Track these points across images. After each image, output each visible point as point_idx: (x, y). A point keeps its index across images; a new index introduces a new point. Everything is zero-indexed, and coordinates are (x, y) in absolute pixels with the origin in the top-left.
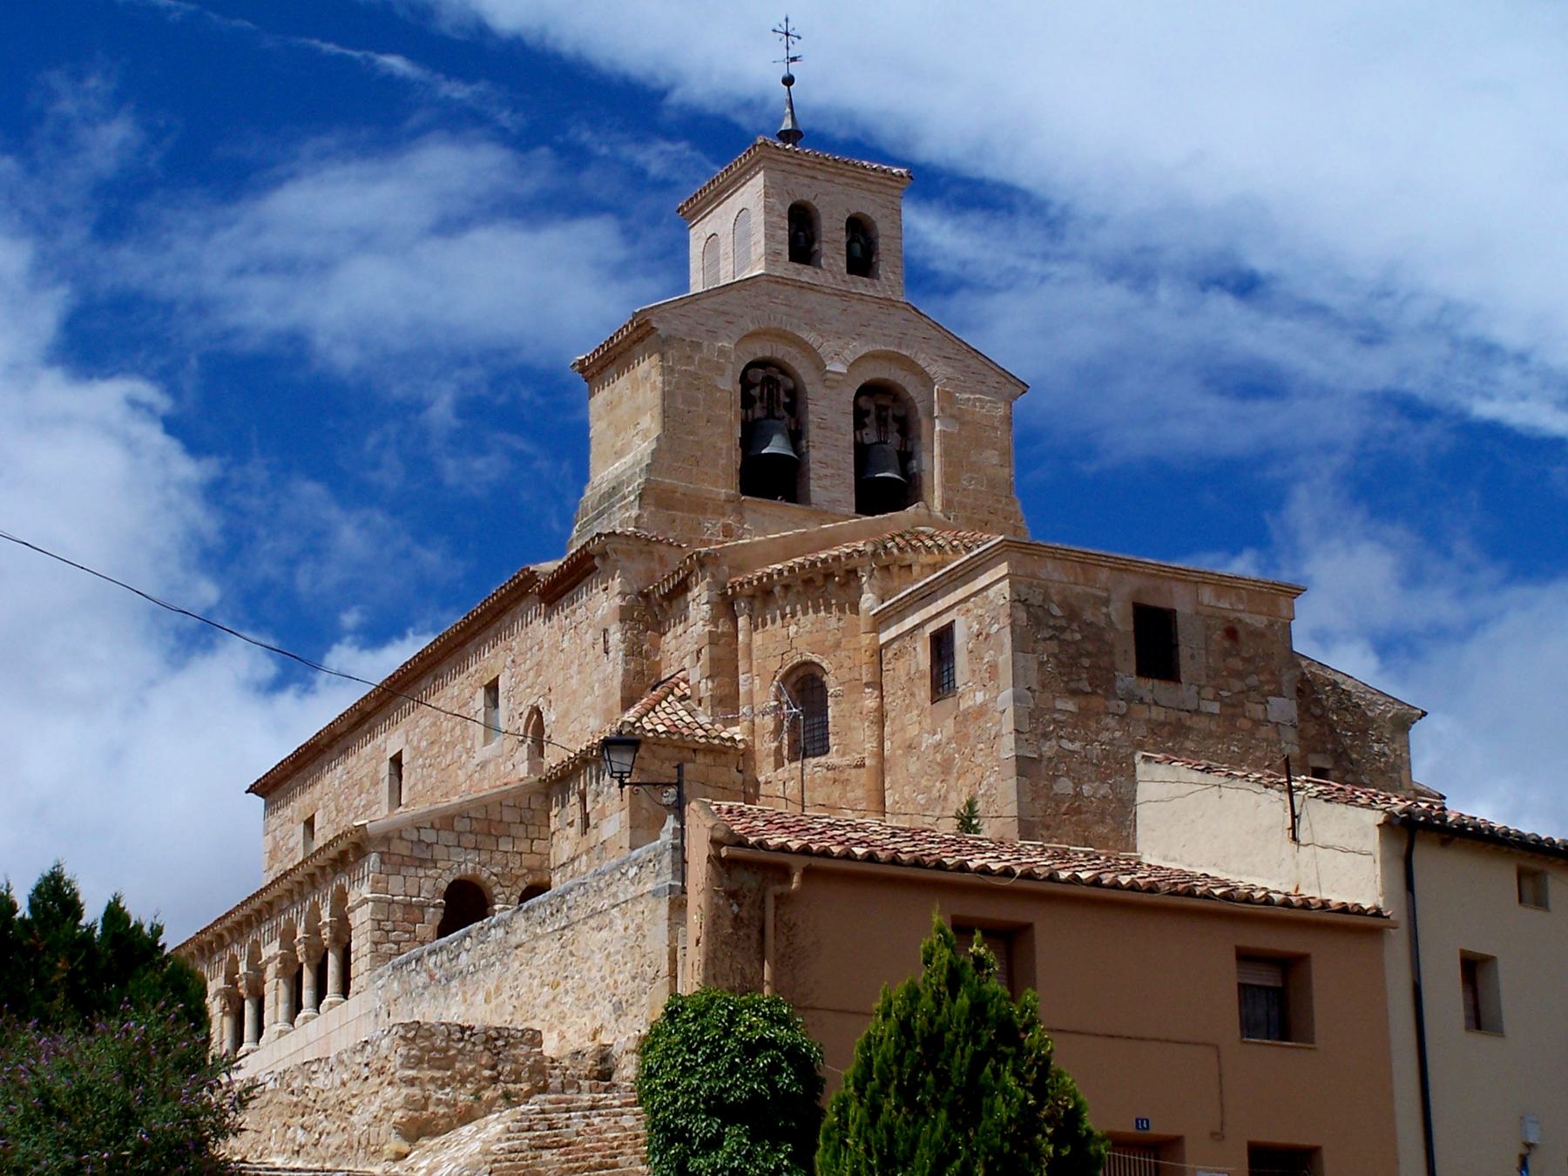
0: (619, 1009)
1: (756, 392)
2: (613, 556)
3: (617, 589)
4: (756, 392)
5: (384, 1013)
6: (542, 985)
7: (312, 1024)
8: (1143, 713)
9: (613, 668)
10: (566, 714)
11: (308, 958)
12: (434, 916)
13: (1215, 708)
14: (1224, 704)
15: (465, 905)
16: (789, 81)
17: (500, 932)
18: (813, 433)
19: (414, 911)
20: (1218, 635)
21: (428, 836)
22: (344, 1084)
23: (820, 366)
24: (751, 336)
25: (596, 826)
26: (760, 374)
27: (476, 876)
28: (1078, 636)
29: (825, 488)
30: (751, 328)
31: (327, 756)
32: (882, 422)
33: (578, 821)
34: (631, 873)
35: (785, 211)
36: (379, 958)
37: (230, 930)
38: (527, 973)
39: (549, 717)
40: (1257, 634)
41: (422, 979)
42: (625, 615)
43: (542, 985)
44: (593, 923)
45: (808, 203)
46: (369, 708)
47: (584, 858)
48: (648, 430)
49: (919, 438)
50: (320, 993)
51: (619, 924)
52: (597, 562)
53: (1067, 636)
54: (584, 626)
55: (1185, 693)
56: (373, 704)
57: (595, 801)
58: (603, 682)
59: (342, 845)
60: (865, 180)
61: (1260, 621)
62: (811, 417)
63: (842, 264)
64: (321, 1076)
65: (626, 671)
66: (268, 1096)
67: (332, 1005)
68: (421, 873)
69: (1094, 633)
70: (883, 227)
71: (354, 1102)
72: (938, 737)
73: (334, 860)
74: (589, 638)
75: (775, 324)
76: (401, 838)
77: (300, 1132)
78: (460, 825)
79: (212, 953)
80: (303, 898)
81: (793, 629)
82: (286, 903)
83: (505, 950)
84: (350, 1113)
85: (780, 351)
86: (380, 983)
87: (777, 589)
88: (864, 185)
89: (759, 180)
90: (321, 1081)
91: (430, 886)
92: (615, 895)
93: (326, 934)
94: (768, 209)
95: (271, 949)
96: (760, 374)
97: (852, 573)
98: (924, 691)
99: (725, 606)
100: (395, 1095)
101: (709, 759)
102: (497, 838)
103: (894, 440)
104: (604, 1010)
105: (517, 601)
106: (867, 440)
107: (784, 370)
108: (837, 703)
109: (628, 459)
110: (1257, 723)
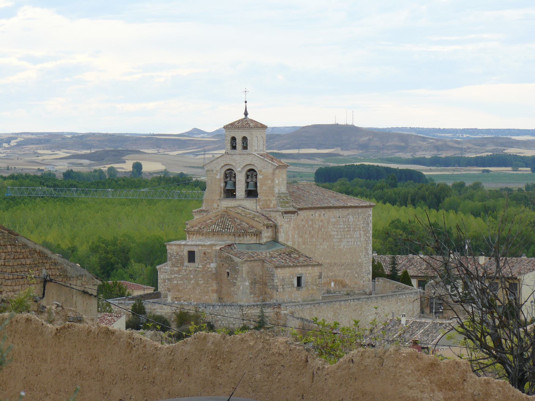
1: (228, 175)
4: (228, 175)
13: (201, 266)
14: (203, 265)
16: (246, 102)
32: (252, 177)
40: (209, 253)
55: (196, 265)
61: (210, 251)
69: (181, 257)
110: (208, 268)
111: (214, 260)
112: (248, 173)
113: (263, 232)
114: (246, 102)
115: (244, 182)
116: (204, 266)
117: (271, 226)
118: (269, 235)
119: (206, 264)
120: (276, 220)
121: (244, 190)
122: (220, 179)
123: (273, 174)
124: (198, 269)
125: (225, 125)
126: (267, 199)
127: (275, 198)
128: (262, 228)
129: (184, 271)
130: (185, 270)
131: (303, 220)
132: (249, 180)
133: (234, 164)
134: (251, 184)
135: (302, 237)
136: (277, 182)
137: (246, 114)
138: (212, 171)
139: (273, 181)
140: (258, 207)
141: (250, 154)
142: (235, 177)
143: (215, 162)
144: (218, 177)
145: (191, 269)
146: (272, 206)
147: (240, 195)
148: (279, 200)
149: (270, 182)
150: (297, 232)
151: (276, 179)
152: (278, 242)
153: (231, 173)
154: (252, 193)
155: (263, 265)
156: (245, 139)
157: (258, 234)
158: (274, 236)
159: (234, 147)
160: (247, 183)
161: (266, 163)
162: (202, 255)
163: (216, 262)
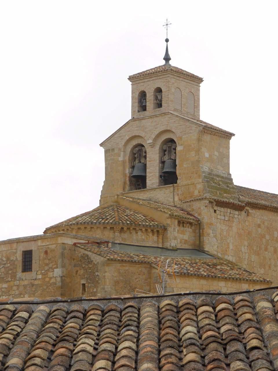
4: (136, 156)
8: (23, 283)
13: (40, 277)
14: (42, 274)
16: (167, 40)
28: (9, 265)
29: (150, 180)
53: (6, 266)
60: (158, 76)
61: (53, 247)
88: (158, 77)
110: (51, 278)
111: (60, 261)
113: (170, 229)
114: (167, 40)
115: (158, 161)
116: (45, 275)
117: (191, 224)
118: (186, 237)
119: (48, 270)
120: (200, 214)
122: (124, 162)
123: (199, 140)
124: (36, 282)
125: (132, 74)
126: (189, 182)
127: (200, 180)
128: (169, 221)
130: (18, 286)
131: (259, 226)
132: (166, 158)
133: (142, 134)
134: (168, 162)
135: (258, 254)
136: (207, 155)
137: (167, 58)
139: (198, 151)
140: (176, 199)
141: (165, 114)
142: (145, 157)
144: (121, 159)
145: (26, 283)
146: (196, 193)
147: (153, 184)
148: (207, 182)
149: (193, 154)
150: (246, 243)
151: (203, 149)
152: (204, 252)
153: (140, 150)
154: (169, 178)
155: (150, 273)
157: (160, 231)
158: (198, 242)
160: (163, 162)
161: (188, 124)
162: (42, 255)
163: (63, 266)
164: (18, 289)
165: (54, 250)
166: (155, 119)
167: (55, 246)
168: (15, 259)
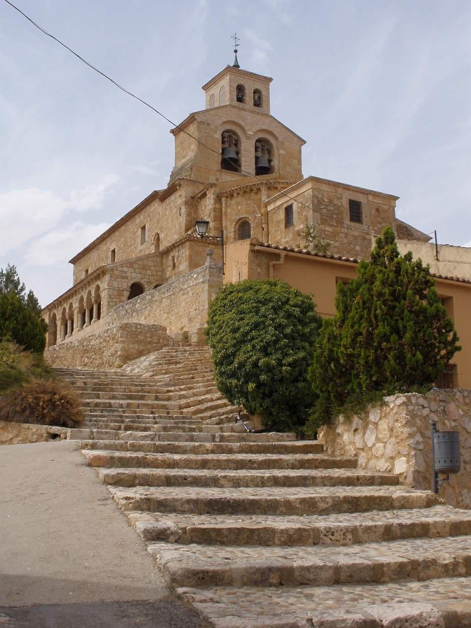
0: (190, 320)
1: (226, 139)
2: (183, 185)
3: (184, 196)
4: (226, 139)
5: (111, 324)
6: (164, 313)
7: (89, 327)
8: (351, 233)
9: (183, 220)
10: (167, 235)
11: (87, 308)
12: (126, 294)
15: (136, 290)
16: (236, 51)
17: (150, 297)
18: (243, 152)
19: (120, 292)
20: (373, 211)
21: (125, 269)
22: (101, 343)
23: (244, 131)
24: (224, 123)
25: (178, 267)
26: (227, 134)
27: (140, 282)
28: (332, 208)
30: (225, 120)
31: (93, 251)
32: (263, 150)
33: (172, 266)
34: (195, 276)
35: (236, 87)
36: (110, 306)
37: (64, 300)
38: (159, 309)
39: (162, 236)
40: (384, 211)
41: (124, 312)
42: (186, 203)
43: (164, 313)
44: (181, 293)
45: (242, 85)
46: (105, 236)
47: (174, 277)
48: (194, 149)
49: (274, 155)
50: (91, 318)
51: (191, 294)
52: (178, 188)
54: (173, 207)
56: (107, 235)
57: (178, 259)
58: (179, 224)
59: (98, 272)
61: (386, 207)
62: (242, 148)
63: (252, 103)
64: (93, 341)
65: (186, 220)
66: (76, 348)
67: (95, 321)
68: (123, 280)
69: (338, 207)
70: (264, 93)
71: (105, 349)
72: (287, 239)
73: (96, 277)
74: (174, 211)
75: (232, 119)
76: (117, 270)
77: (86, 359)
78: (135, 266)
79: (58, 306)
80: (86, 288)
81: (240, 207)
82: (81, 291)
83: (151, 302)
84: (103, 352)
85: (233, 128)
86: (110, 314)
87: (235, 195)
89: (228, 77)
90: (93, 342)
91: (126, 285)
92: (189, 284)
93: (93, 300)
94: (230, 86)
95: (76, 305)
96: (227, 134)
97: (259, 189)
98: (283, 226)
99: (218, 199)
100: (119, 346)
101: (213, 247)
102: (147, 270)
103: (266, 157)
104: (185, 321)
105: (152, 202)
106: (258, 156)
107: (235, 134)
108: (254, 230)
109: (188, 158)
112: (259, 144)
114: (236, 51)
121: (254, 166)
129: (342, 235)
138: (209, 124)
143: (212, 112)
145: (356, 233)
156: (256, 92)
159: (240, 100)
160: (257, 158)
164: (346, 237)
165: (387, 211)
166: (256, 116)
167: (388, 207)
168: (340, 204)
